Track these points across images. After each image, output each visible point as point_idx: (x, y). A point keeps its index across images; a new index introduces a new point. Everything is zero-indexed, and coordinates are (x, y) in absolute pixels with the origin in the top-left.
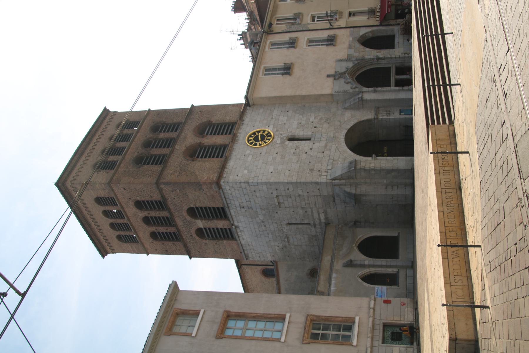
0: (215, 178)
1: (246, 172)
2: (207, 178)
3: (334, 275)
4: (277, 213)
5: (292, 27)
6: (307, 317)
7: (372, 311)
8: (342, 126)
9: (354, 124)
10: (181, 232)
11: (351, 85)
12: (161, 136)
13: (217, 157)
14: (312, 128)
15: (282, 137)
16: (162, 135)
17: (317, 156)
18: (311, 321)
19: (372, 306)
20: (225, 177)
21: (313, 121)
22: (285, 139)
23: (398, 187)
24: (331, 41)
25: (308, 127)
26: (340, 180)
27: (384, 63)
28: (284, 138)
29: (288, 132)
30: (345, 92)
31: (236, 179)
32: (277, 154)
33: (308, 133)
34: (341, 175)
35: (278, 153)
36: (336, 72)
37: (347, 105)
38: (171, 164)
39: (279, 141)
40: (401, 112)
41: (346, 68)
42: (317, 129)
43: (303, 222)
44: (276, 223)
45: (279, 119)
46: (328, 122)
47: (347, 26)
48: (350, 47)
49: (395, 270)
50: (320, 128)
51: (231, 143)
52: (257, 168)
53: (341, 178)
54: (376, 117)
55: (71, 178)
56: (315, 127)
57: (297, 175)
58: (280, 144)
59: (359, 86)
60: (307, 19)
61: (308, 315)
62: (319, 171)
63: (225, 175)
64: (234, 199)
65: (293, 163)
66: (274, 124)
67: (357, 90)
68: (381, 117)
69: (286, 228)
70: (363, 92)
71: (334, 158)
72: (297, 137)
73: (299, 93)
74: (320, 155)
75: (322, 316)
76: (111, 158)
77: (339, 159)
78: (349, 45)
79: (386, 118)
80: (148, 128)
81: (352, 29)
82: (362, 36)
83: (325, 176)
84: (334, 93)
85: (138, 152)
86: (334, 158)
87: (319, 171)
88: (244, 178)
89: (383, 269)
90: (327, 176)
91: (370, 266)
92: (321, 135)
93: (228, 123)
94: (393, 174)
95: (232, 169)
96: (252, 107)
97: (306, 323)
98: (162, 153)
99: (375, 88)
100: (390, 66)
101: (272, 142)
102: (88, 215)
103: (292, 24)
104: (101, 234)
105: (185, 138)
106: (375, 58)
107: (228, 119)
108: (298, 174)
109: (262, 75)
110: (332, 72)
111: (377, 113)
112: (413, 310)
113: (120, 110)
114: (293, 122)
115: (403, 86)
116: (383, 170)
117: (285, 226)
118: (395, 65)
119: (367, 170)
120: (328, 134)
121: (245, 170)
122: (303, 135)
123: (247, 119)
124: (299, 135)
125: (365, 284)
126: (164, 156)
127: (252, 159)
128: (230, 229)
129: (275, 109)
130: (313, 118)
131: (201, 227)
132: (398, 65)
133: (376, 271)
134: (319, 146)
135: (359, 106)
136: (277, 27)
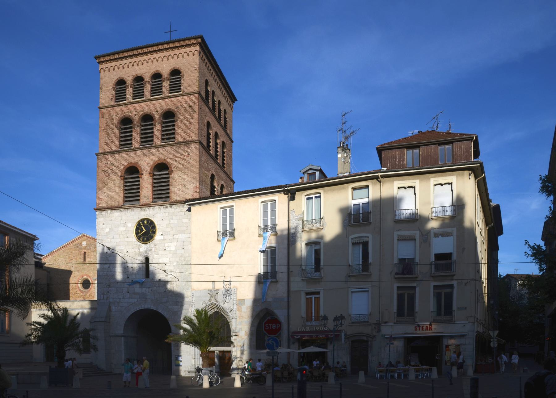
1: (107, 230)
2: (101, 198)
9: (164, 315)
28: (146, 254)
50: (158, 285)
63: (104, 213)
66: (164, 239)
71: (122, 302)
83: (103, 297)
86: (122, 302)
87: (108, 292)
88: (100, 231)
114: (167, 258)
120: (151, 293)
121: (109, 228)
127: (121, 231)
134: (135, 288)
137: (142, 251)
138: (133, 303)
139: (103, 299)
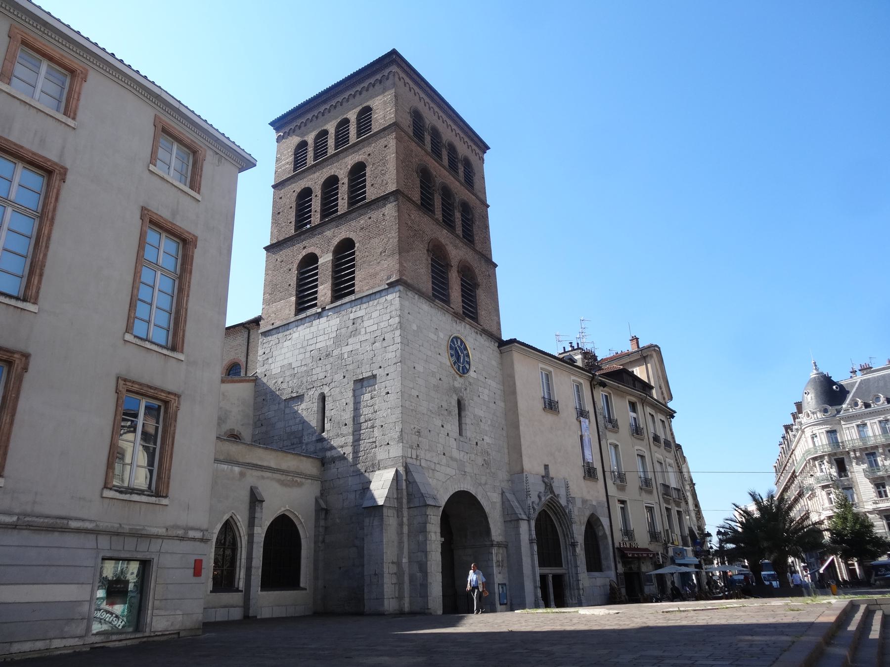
0: (405, 278)
2: (405, 267)
3: (237, 469)
4: (344, 377)
5: (602, 417)
6: (175, 395)
7: (180, 532)
8: (480, 487)
10: (311, 232)
11: (537, 502)
12: (458, 214)
13: (433, 289)
14: (475, 438)
15: (463, 390)
16: (458, 215)
17: (439, 443)
18: (166, 403)
19: (191, 534)
20: (407, 295)
21: (485, 440)
22: (461, 394)
23: (395, 584)
24: (590, 472)
25: (477, 433)
26: (406, 480)
27: (567, 556)
28: (461, 393)
29: (469, 400)
30: (528, 494)
31: (404, 311)
32: (440, 379)
33: (469, 432)
34: (415, 482)
35: (441, 380)
36: (552, 478)
37: (509, 496)
38: (423, 217)
39: (457, 384)
40: (503, 585)
41: (558, 495)
42: (475, 446)
43: (326, 422)
44: (326, 377)
45: (485, 388)
46: (485, 465)
47: (609, 497)
48: (584, 501)
49: (241, 585)
51: (453, 311)
52: (420, 346)
53: (409, 481)
54: (495, 543)
55: (402, 75)
56: (477, 443)
57: (411, 408)
58: (453, 385)
59: (534, 516)
60: (611, 438)
61: (178, 396)
62: (418, 445)
64: (368, 309)
65: (428, 403)
67: (532, 511)
68: (494, 551)
69: (314, 394)
70: (529, 521)
71: (438, 471)
72: (463, 414)
73: (522, 421)
74: (440, 449)
75: (175, 426)
76: (428, 138)
77: (436, 479)
78: (587, 500)
79: (493, 560)
80: (466, 199)
81: (606, 506)
82: (598, 519)
84: (525, 474)
85: (436, 176)
86: (438, 471)
88: (405, 323)
89: (244, 561)
90: (411, 458)
91: (251, 536)
92: (467, 452)
93: (477, 313)
94: (419, 574)
95: (417, 306)
96: (498, 351)
97: (162, 391)
98: (436, 210)
99: (536, 541)
100: (564, 566)
101: (455, 373)
102: (342, 98)
103: (605, 417)
104: (310, 118)
105: (456, 247)
106: (574, 540)
107: (482, 313)
108: (412, 410)
109: (541, 369)
110: (552, 473)
111: (499, 545)
112: (177, 627)
113: (486, 166)
115: (541, 588)
116: (426, 557)
117: (319, 391)
118: (566, 573)
119: (425, 527)
122: (466, 424)
123: (483, 340)
124: (465, 417)
125: (219, 526)
126: (433, 212)
128: (315, 305)
129: (497, 383)
130: (488, 442)
131: (319, 260)
132: (567, 578)
133: (241, 547)
135: (507, 514)
136: (600, 393)
137: (457, 386)
138: (451, 476)
139: (411, 458)
